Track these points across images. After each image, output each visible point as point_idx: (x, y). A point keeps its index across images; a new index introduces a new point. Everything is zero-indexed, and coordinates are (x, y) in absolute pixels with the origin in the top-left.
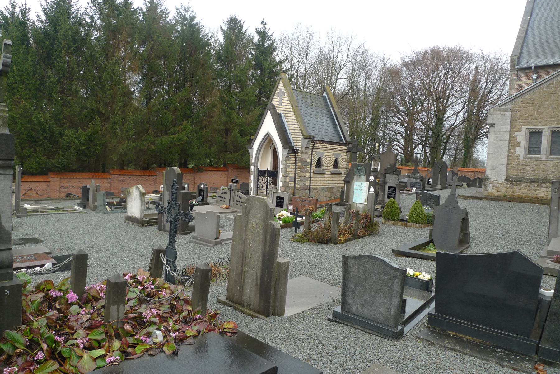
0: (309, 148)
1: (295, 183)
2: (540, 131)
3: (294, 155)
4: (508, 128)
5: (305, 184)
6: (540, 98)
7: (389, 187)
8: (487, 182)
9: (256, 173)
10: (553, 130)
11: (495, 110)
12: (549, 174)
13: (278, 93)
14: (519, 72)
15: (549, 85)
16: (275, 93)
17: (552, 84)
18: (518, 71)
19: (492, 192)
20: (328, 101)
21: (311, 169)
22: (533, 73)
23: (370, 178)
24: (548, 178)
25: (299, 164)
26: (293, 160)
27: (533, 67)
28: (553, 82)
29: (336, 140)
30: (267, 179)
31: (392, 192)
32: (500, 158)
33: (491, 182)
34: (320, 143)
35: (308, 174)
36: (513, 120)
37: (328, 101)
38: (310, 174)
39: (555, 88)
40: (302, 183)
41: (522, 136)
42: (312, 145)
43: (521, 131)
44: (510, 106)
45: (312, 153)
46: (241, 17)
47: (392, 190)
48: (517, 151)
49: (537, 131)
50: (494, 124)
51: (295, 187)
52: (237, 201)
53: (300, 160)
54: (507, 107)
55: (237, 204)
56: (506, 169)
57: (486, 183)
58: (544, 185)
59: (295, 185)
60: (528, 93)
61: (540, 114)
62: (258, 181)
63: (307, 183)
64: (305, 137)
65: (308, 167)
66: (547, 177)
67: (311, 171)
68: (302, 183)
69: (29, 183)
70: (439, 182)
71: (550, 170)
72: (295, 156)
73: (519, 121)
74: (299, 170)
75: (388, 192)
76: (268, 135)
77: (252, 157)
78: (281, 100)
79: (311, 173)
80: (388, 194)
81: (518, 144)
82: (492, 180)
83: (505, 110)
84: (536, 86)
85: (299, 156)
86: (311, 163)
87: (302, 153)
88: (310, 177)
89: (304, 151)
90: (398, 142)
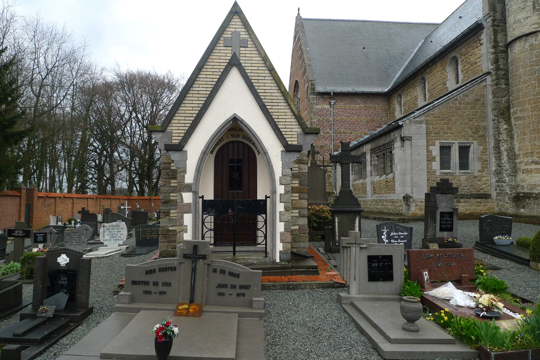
2: (450, 145)
4: (425, 141)
6: (448, 113)
7: (442, 214)
8: (410, 201)
10: (461, 145)
11: (411, 122)
12: (463, 189)
13: (225, 40)
14: (318, 96)
15: (454, 100)
17: (457, 100)
18: (316, 95)
19: (416, 212)
22: (330, 99)
24: (463, 193)
27: (332, 93)
28: (457, 98)
31: (447, 221)
32: (420, 174)
33: (414, 201)
36: (428, 133)
39: (460, 104)
41: (436, 151)
43: (434, 145)
44: (423, 118)
48: (433, 166)
49: (447, 146)
52: (219, 286)
55: (222, 294)
56: (427, 186)
58: (462, 200)
60: (439, 107)
61: (450, 129)
66: (462, 192)
71: (463, 185)
73: (432, 135)
75: (441, 221)
77: (185, 171)
80: (441, 224)
81: (434, 159)
82: (414, 198)
83: (421, 122)
84: (445, 100)
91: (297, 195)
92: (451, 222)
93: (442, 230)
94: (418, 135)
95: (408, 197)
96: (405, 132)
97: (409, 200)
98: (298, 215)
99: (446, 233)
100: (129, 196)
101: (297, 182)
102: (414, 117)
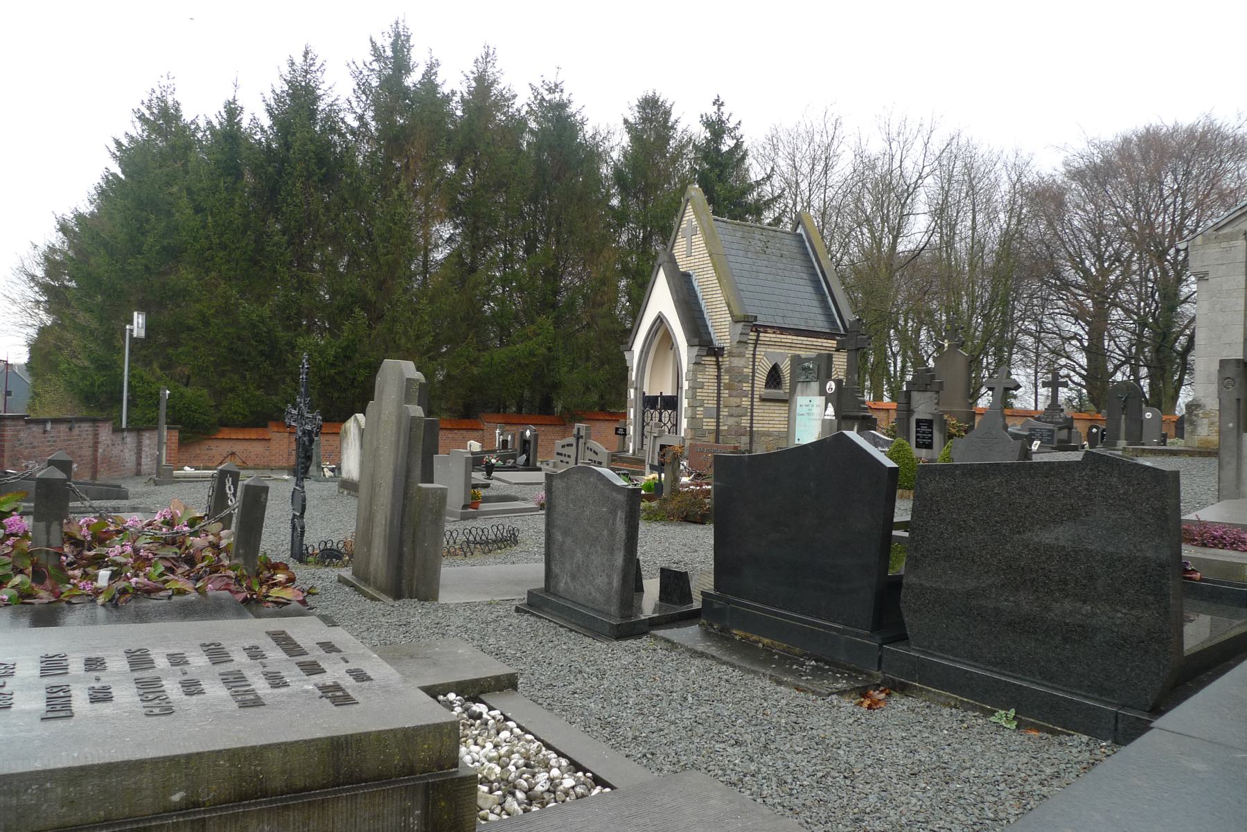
0: (746, 343)
1: (718, 423)
3: (714, 359)
5: (738, 424)
7: (918, 422)
9: (640, 403)
13: (685, 229)
16: (677, 232)
19: (1210, 438)
20: (807, 244)
21: (753, 391)
23: (827, 387)
25: (726, 379)
26: (712, 371)
29: (820, 324)
30: (661, 414)
31: (924, 432)
34: (774, 333)
35: (746, 402)
37: (807, 244)
38: (752, 401)
40: (731, 421)
42: (753, 336)
45: (754, 355)
46: (666, 96)
47: (924, 428)
50: (1206, 273)
51: (718, 431)
53: (728, 371)
54: (1237, 228)
57: (1195, 418)
59: (718, 426)
62: (643, 421)
63: (745, 422)
64: (735, 318)
65: (746, 387)
67: (753, 394)
68: (731, 421)
69: (231, 443)
70: (1122, 434)
72: (717, 361)
74: (725, 393)
75: (917, 432)
76: (660, 320)
77: (632, 370)
78: (690, 244)
79: (752, 398)
80: (917, 437)
82: (1208, 408)
83: (1231, 237)
85: (726, 361)
86: (753, 376)
87: (731, 354)
88: (752, 409)
89: (734, 350)
90: (1068, 358)
91: (727, 391)
92: (930, 435)
93: (918, 446)
94: (1224, 267)
95: (1192, 405)
96: (1195, 264)
97: (1195, 412)
98: (727, 414)
99: (924, 450)
100: (1093, 413)
101: (727, 377)
102: (1216, 227)
